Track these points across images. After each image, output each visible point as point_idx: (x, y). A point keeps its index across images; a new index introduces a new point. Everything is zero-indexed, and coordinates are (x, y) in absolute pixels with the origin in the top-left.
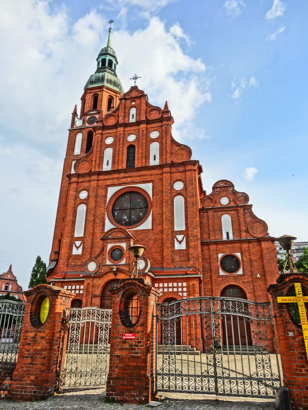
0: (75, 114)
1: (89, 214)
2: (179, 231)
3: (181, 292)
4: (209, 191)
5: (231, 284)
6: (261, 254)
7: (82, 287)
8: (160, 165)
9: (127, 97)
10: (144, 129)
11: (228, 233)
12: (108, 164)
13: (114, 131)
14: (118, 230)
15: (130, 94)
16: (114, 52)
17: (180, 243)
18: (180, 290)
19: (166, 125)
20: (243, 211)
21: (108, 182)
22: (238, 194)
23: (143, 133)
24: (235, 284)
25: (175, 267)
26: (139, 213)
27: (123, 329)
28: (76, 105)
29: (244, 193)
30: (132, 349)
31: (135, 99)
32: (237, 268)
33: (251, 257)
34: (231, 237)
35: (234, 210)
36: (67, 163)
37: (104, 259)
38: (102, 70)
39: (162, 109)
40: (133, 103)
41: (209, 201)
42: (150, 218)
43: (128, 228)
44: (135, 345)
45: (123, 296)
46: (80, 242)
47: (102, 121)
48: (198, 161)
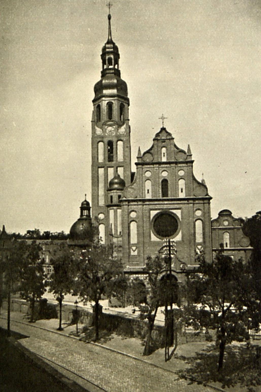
4: (214, 215)
21: (151, 207)
42: (180, 234)
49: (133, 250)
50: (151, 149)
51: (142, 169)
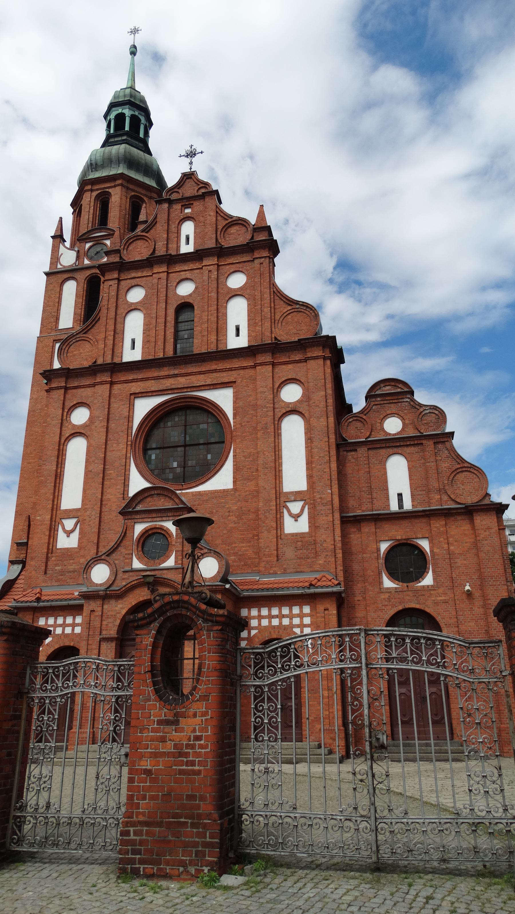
0: (58, 237)
1: (93, 458)
2: (292, 492)
3: (298, 626)
5: (407, 606)
6: (473, 540)
7: (79, 620)
8: (249, 347)
9: (174, 196)
10: (212, 267)
11: (400, 495)
12: (133, 348)
13: (146, 272)
14: (159, 492)
15: (180, 191)
16: (143, 100)
18: (296, 621)
19: (262, 257)
20: (433, 446)
21: (135, 387)
22: (422, 410)
23: (209, 277)
24: (417, 606)
25: (285, 572)
26: (206, 453)
27: (160, 709)
28: (61, 218)
29: (435, 408)
30: (181, 754)
32: (421, 574)
33: (452, 548)
34: (408, 505)
35: (414, 445)
36: (43, 348)
37: (127, 556)
38: (116, 139)
39: (253, 221)
41: (359, 424)
42: (229, 466)
43: (181, 487)
44: (188, 746)
45: (159, 632)
46: (74, 521)
47: (118, 251)
48: (334, 337)
49: (64, 528)
51: (118, 284)
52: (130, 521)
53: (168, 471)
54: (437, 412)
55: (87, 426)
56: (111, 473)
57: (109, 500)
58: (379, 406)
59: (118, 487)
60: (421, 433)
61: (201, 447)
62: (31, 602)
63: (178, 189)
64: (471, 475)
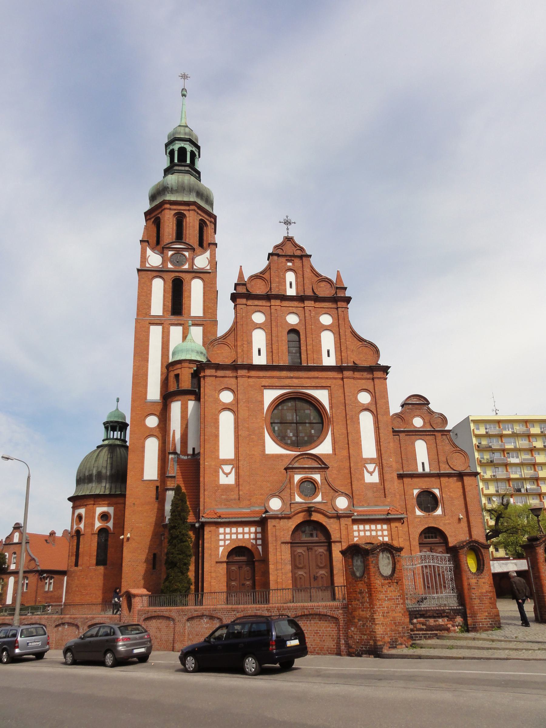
5: (430, 526)
10: (311, 308)
11: (423, 464)
17: (371, 475)
18: (380, 533)
21: (265, 382)
24: (435, 526)
29: (442, 415)
31: (293, 259)
32: (435, 508)
34: (427, 470)
40: (289, 264)
41: (399, 420)
42: (329, 438)
50: (263, 272)
52: (292, 473)
53: (286, 438)
54: (442, 417)
55: (233, 404)
56: (253, 438)
57: (254, 455)
58: (410, 410)
59: (259, 447)
60: (433, 428)
61: (307, 425)
62: (214, 518)
63: (282, 246)
64: (460, 455)
